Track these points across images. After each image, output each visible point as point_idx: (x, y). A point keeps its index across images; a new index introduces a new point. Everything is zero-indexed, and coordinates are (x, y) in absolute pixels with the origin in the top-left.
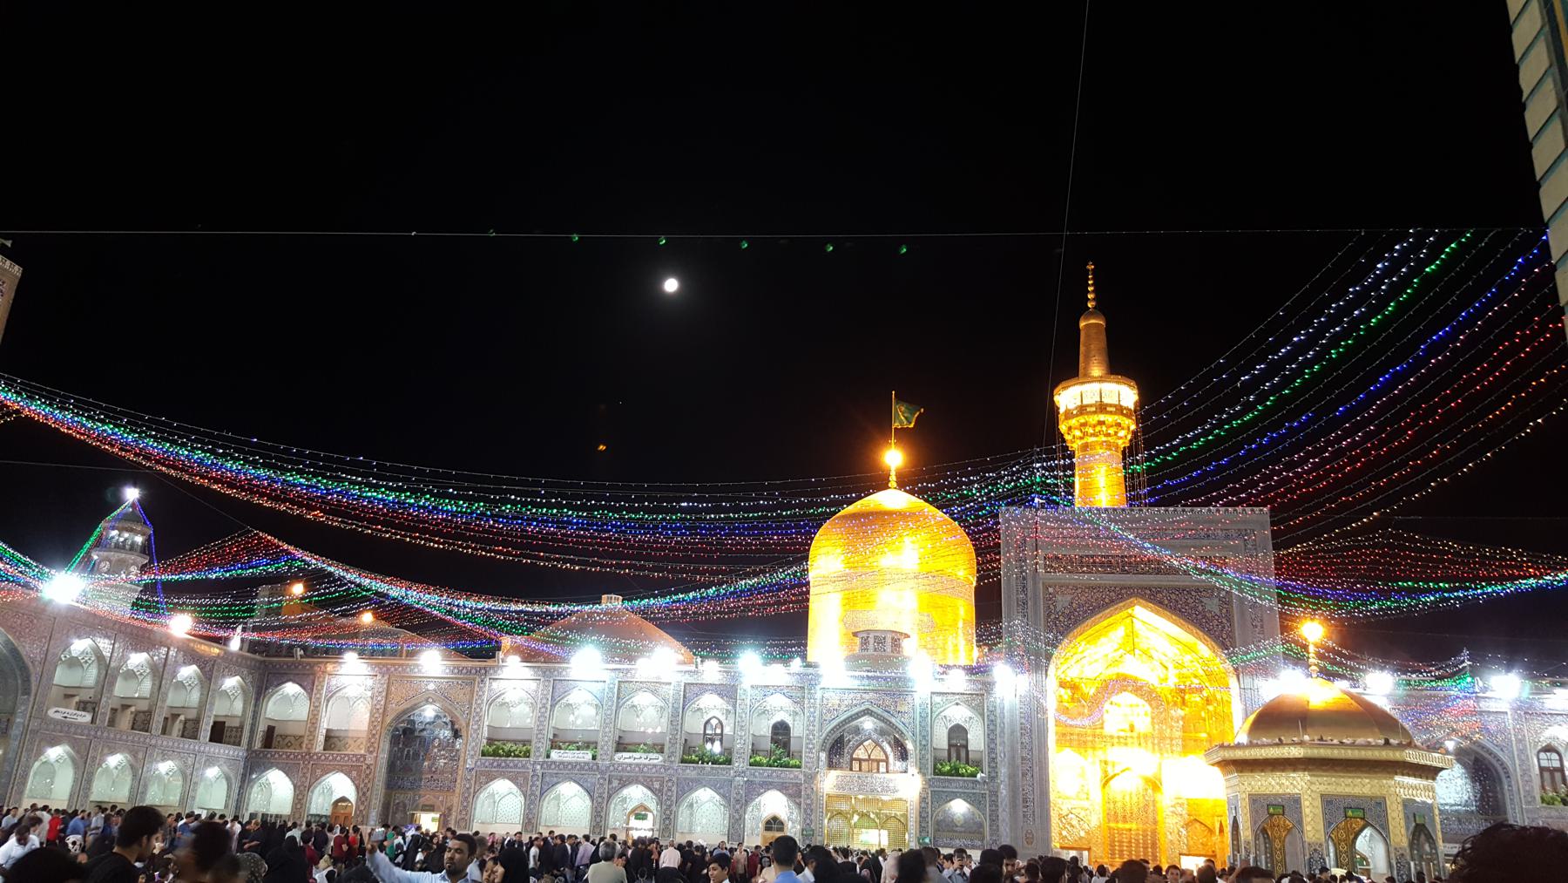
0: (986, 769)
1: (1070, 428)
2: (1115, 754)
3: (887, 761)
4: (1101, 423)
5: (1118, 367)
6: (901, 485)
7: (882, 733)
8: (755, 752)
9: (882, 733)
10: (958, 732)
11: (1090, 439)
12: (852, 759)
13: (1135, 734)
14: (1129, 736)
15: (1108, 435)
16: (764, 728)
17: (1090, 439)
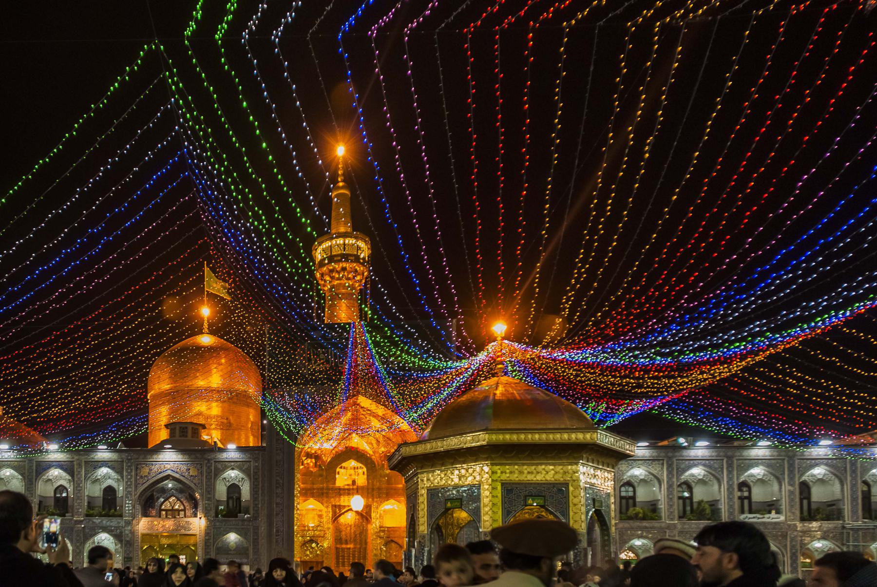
0: (252, 512)
1: (322, 275)
2: (344, 501)
3: (184, 510)
4: (344, 269)
7: (181, 491)
8: (90, 506)
9: (181, 491)
10: (233, 489)
11: (336, 282)
12: (161, 510)
13: (355, 487)
14: (352, 489)
15: (348, 279)
16: (97, 491)
17: (336, 282)
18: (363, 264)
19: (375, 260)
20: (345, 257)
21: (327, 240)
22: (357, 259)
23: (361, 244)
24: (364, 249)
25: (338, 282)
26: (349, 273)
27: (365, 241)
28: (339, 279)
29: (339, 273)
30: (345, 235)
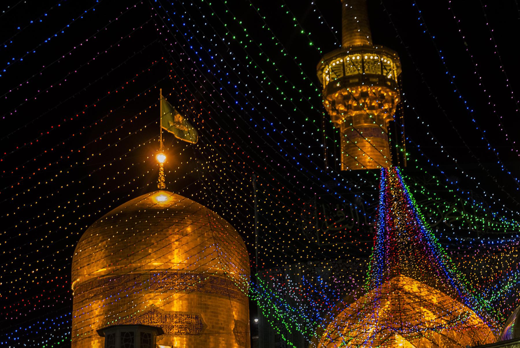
1: (333, 103)
4: (364, 95)
5: (381, 41)
6: (171, 188)
15: (371, 108)
18: (391, 88)
19: (405, 83)
20: (365, 79)
21: (337, 57)
22: (382, 81)
23: (387, 61)
24: (392, 69)
25: (358, 112)
26: (371, 100)
27: (392, 58)
28: (357, 108)
29: (356, 100)
30: (362, 50)
